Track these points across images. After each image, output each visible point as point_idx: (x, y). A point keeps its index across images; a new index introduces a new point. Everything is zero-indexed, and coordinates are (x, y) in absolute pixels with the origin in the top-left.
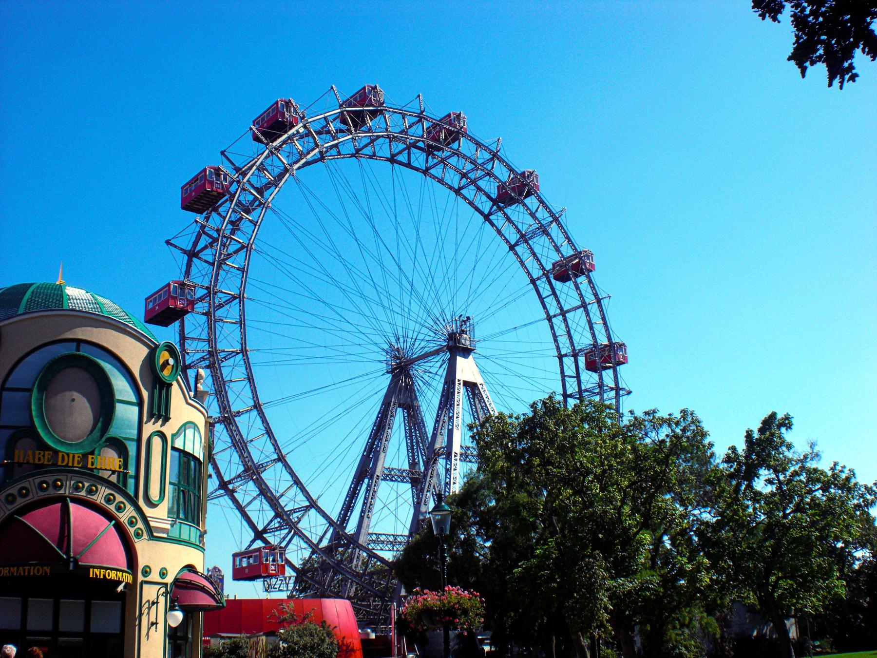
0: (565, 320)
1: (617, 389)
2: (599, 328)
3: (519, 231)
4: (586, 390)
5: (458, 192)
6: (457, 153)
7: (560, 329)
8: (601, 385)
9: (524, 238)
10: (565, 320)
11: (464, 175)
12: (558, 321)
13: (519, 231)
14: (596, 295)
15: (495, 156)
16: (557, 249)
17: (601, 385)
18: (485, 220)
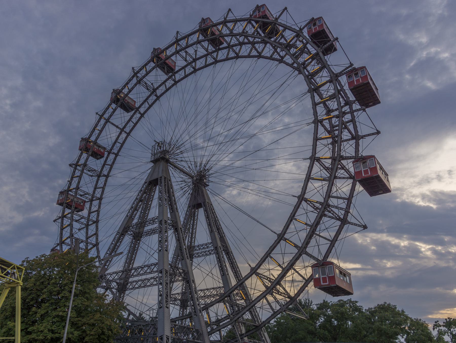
0: (157, 88)
1: (177, 41)
2: (149, 68)
3: (120, 134)
4: (186, 60)
5: (107, 176)
6: (77, 188)
7: (163, 88)
8: (177, 52)
9: (122, 130)
10: (157, 88)
11: (99, 176)
12: (159, 92)
13: (120, 134)
14: (133, 77)
15: (77, 165)
16: (115, 110)
17: (177, 52)
18: (118, 155)
